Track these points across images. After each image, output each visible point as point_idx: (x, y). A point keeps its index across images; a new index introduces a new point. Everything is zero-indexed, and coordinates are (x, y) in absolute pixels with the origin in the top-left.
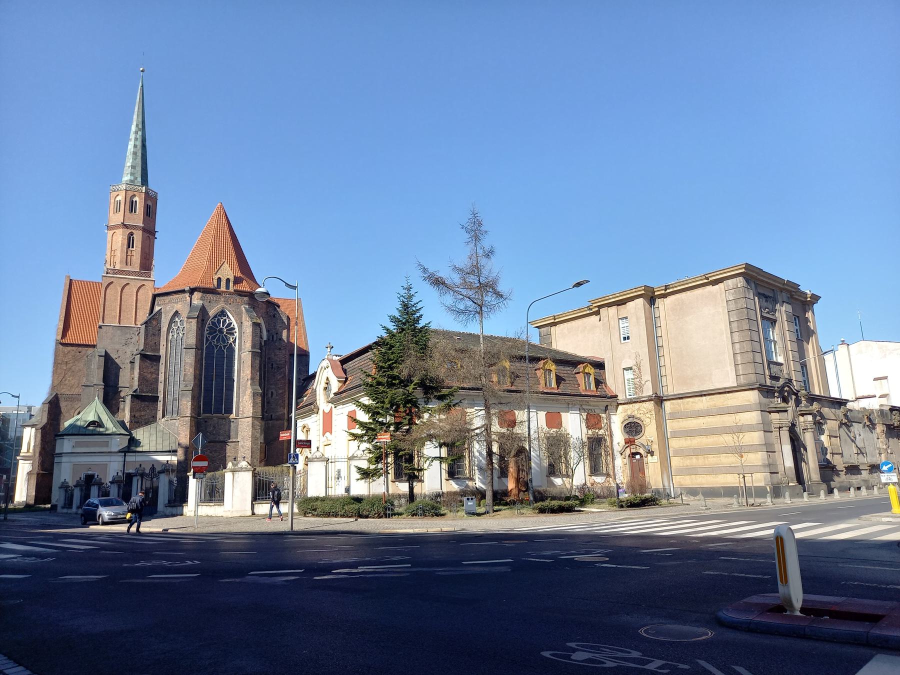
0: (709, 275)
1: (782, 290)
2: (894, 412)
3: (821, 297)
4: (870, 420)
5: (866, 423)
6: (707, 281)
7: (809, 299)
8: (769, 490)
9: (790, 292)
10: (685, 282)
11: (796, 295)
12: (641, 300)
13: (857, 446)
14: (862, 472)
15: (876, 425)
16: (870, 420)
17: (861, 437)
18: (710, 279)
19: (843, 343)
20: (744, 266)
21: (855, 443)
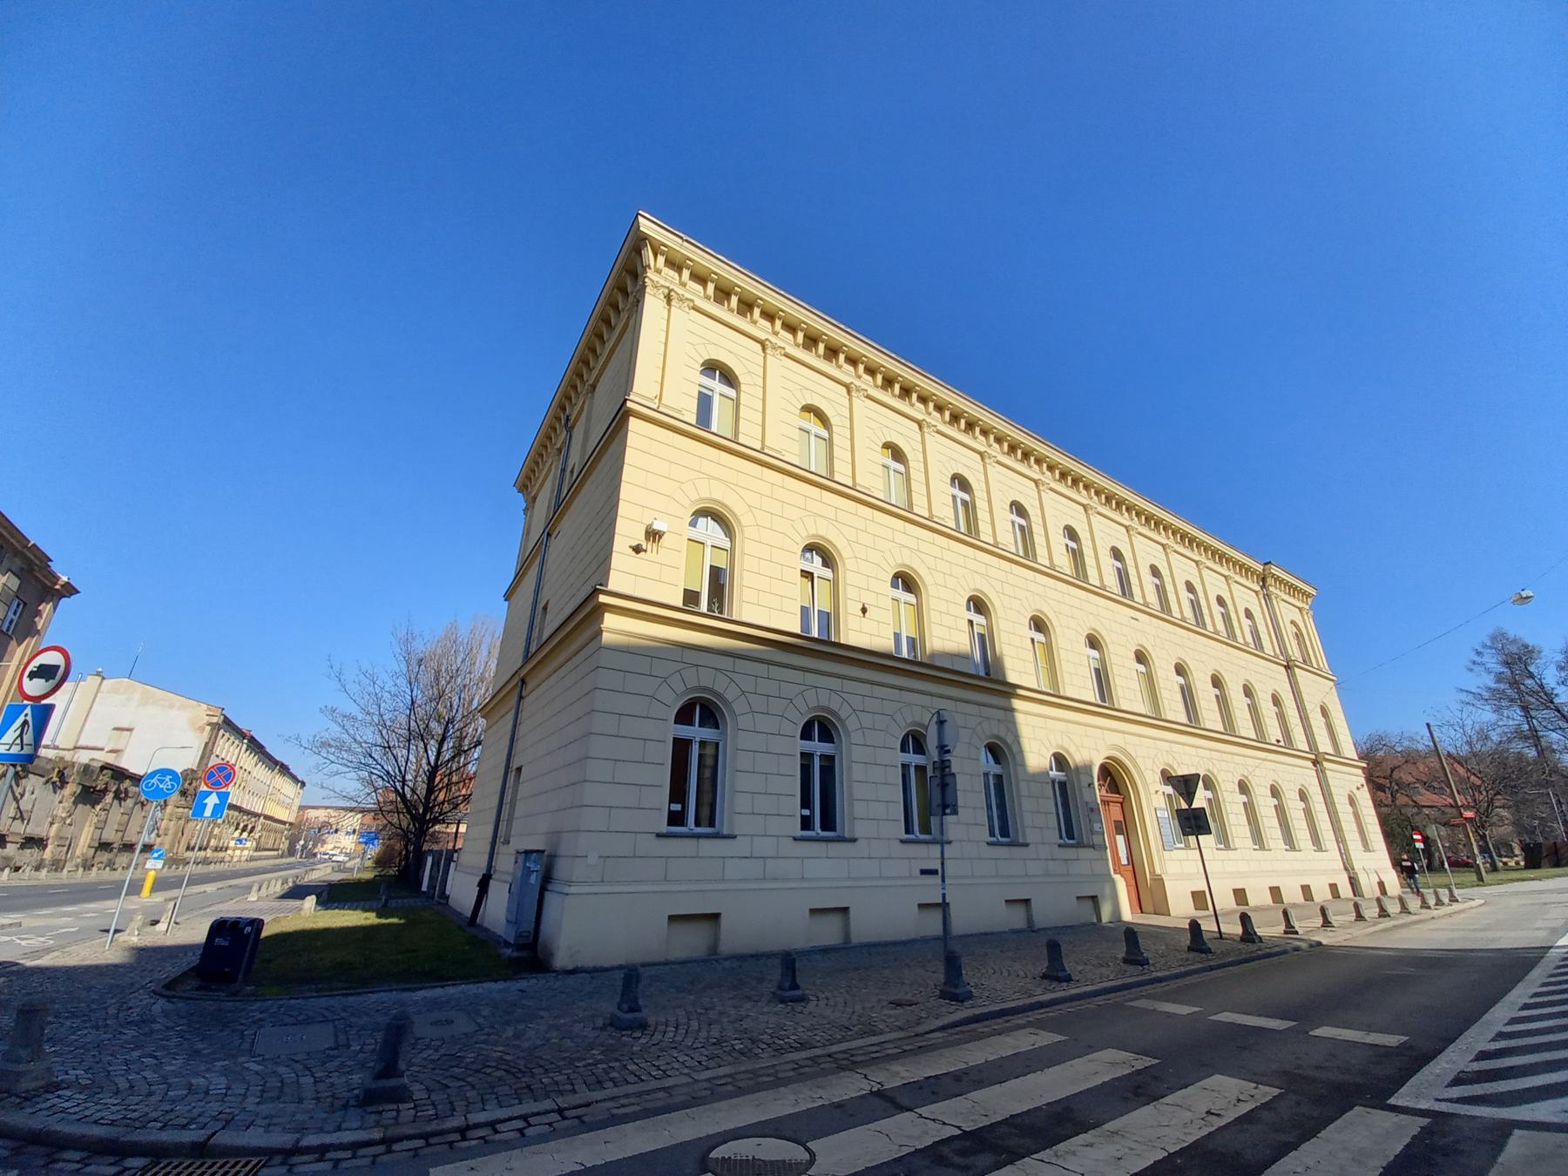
1: (16, 553)
2: (105, 772)
3: (78, 592)
4: (61, 774)
5: (52, 778)
7: (57, 587)
9: (30, 562)
11: (39, 571)
13: (18, 808)
14: (8, 845)
15: (67, 783)
16: (61, 774)
17: (34, 796)
19: (98, 674)
21: (18, 803)
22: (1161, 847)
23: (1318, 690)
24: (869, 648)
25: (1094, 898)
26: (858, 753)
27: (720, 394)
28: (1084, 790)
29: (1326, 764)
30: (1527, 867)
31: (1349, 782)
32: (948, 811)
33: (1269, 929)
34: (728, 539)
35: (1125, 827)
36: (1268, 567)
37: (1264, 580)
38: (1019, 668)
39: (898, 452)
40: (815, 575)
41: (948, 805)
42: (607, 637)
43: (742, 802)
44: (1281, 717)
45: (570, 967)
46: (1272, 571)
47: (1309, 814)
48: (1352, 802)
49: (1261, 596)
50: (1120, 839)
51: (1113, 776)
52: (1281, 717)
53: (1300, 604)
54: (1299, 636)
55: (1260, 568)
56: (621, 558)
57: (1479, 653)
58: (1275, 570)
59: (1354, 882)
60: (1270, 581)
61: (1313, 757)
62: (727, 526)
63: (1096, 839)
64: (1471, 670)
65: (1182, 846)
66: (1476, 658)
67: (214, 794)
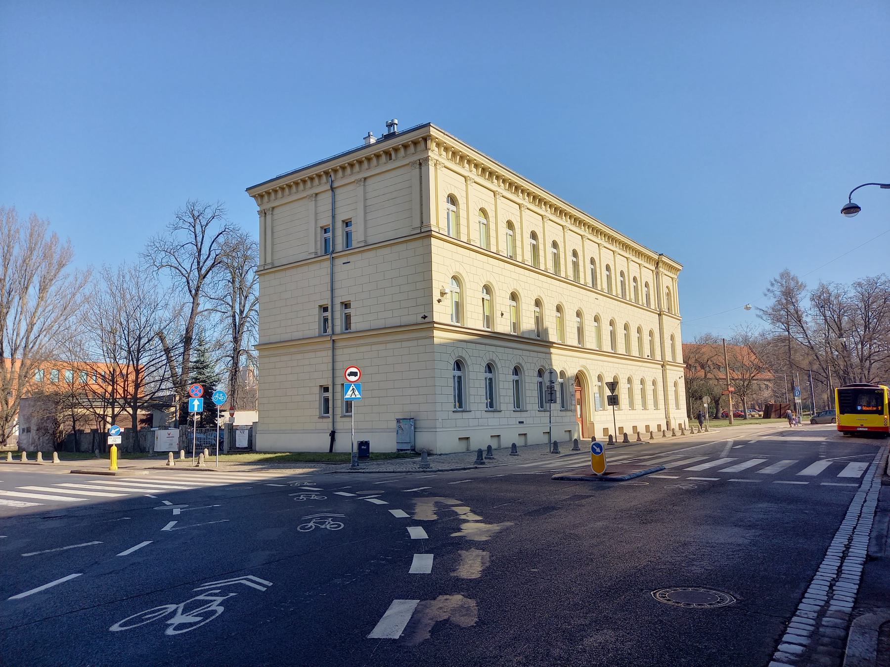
22: (594, 410)
23: (672, 326)
25: (570, 431)
29: (668, 367)
30: (764, 418)
31: (677, 375)
33: (632, 439)
35: (581, 402)
36: (661, 256)
37: (657, 264)
38: (553, 337)
42: (436, 341)
43: (472, 399)
44: (652, 343)
46: (663, 259)
47: (655, 391)
48: (675, 384)
49: (655, 273)
50: (578, 407)
51: (579, 379)
52: (652, 343)
53: (673, 276)
54: (668, 294)
55: (656, 257)
56: (436, 306)
57: (772, 285)
58: (664, 259)
59: (668, 424)
60: (660, 264)
61: (662, 363)
63: (573, 408)
64: (766, 295)
65: (602, 409)
66: (771, 288)
67: (196, 400)
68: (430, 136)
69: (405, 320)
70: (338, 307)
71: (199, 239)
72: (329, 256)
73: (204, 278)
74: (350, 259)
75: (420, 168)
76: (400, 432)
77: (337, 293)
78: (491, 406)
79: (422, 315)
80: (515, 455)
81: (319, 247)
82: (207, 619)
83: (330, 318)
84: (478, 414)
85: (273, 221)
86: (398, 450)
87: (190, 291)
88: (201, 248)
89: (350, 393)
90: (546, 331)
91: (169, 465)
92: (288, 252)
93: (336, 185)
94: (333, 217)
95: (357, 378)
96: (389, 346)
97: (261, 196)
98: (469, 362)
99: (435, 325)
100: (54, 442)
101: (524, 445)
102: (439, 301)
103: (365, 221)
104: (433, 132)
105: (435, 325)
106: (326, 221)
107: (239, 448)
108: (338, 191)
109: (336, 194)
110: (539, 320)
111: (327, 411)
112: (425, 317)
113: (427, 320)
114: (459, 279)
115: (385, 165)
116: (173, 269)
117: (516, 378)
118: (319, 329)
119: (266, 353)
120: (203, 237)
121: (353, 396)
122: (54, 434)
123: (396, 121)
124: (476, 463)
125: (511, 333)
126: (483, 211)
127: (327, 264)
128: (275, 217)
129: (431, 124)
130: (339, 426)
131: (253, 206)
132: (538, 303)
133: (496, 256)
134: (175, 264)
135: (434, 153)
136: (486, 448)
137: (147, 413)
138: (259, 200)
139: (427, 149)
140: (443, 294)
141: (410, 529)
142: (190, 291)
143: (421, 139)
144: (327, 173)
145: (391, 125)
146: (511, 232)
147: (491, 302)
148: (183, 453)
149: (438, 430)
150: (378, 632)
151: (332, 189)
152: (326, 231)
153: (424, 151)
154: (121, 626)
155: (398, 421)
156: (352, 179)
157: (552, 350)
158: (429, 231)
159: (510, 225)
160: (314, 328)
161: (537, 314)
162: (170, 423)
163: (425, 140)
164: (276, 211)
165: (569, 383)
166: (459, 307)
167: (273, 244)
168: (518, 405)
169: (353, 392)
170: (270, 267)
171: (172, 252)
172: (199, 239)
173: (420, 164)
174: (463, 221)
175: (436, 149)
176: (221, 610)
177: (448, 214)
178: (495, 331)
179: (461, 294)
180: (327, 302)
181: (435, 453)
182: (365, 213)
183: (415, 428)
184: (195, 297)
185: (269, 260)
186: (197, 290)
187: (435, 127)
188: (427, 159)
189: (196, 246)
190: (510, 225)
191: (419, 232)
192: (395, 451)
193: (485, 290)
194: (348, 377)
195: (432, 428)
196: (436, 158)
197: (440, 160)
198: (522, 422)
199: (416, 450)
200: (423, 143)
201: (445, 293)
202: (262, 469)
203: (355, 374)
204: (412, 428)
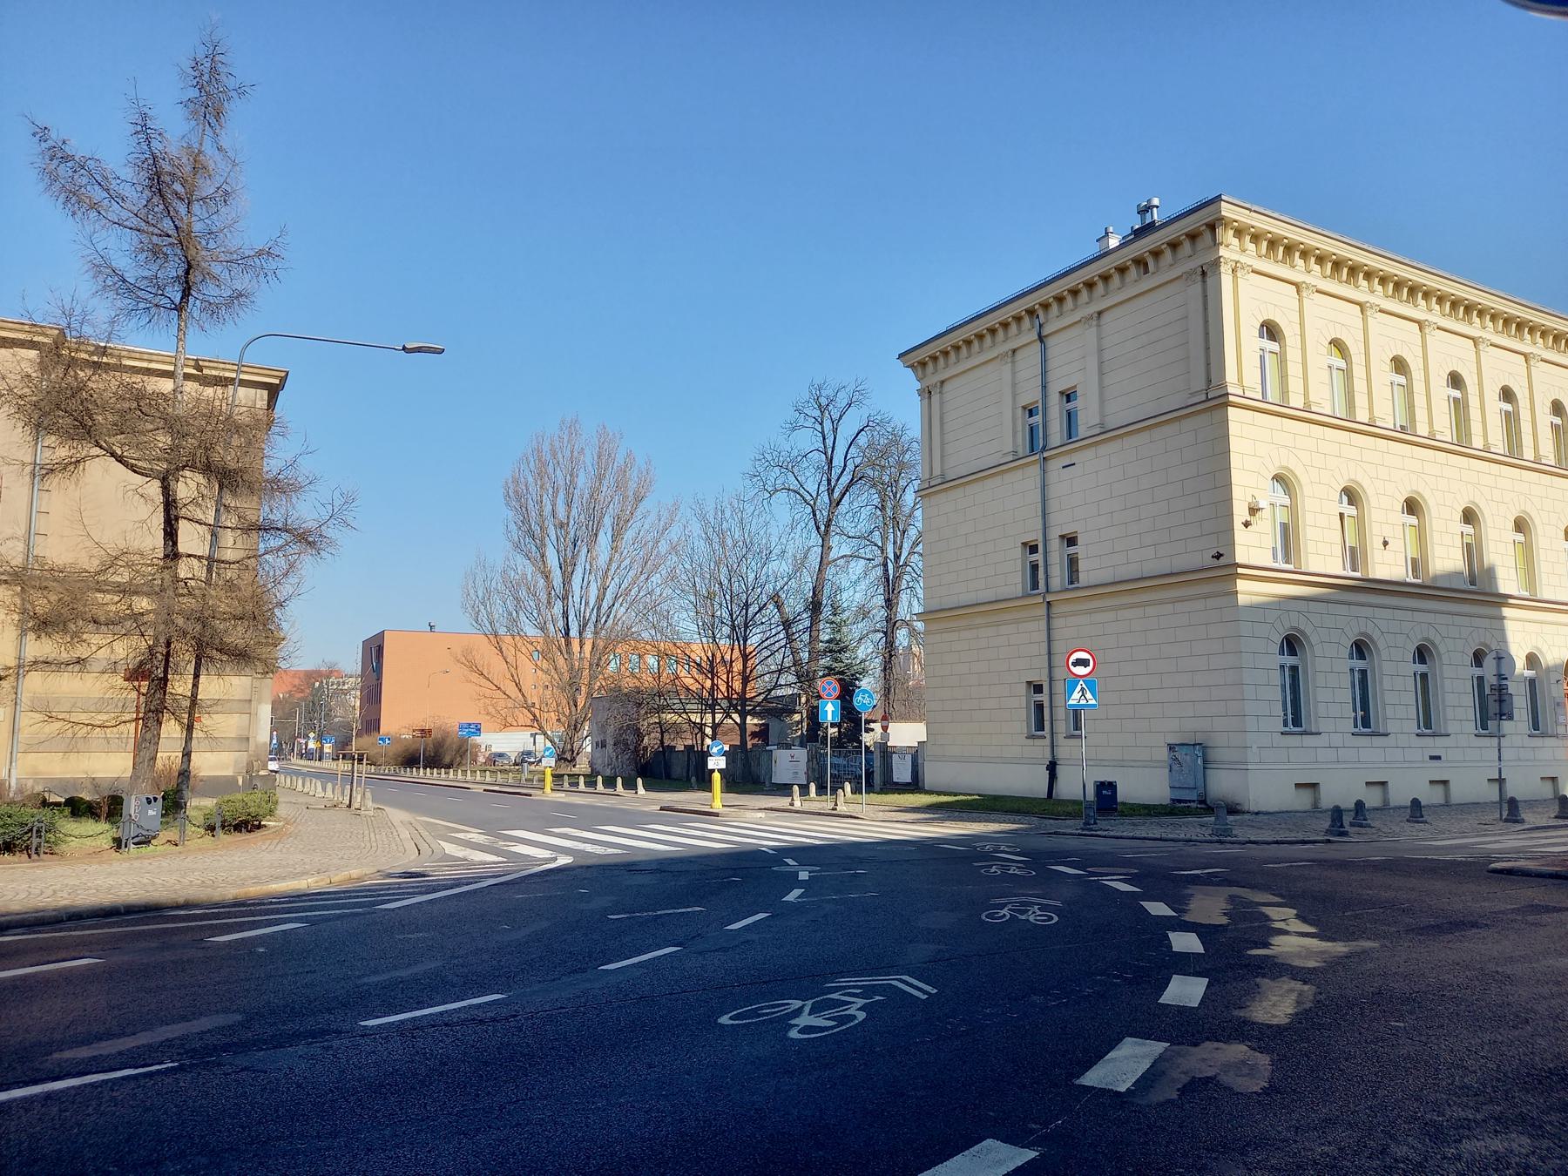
0: (207, 364)
6: (194, 372)
8: (240, 782)
10: (146, 357)
12: (33, 354)
18: (206, 371)
20: (283, 374)
24: (1389, 579)
26: (1388, 668)
27: (1270, 352)
28: (1552, 686)
32: (1504, 717)
34: (1287, 497)
38: (1507, 582)
39: (1400, 362)
40: (1346, 515)
41: (1505, 713)
42: (1242, 599)
45: (1256, 811)
56: (1240, 534)
62: (1287, 485)
67: (830, 704)
68: (1222, 218)
69: (1180, 563)
70: (1055, 544)
71: (829, 442)
72: (1037, 457)
73: (838, 504)
74: (1074, 458)
75: (1204, 282)
76: (1176, 767)
77: (1053, 519)
78: (1366, 722)
79: (1214, 552)
80: (1418, 822)
81: (1020, 441)
82: (842, 1025)
83: (1041, 564)
84: (1337, 740)
85: (942, 403)
86: (1173, 800)
87: (818, 528)
88: (832, 457)
89: (1076, 695)
90: (1490, 573)
91: (792, 805)
92: (964, 455)
93: (1045, 332)
94: (1044, 387)
95: (1087, 670)
96: (1151, 610)
97: (923, 364)
98: (1314, 639)
99: (1240, 570)
100: (636, 763)
101: (1443, 802)
102: (1247, 524)
103: (1102, 387)
104: (1227, 210)
105: (1240, 570)
106: (1031, 395)
107: (897, 783)
108: (1050, 342)
109: (1048, 346)
110: (1472, 551)
111: (1040, 727)
112: (1218, 556)
113: (1222, 561)
114: (1288, 481)
115: (1136, 283)
116: (792, 494)
117: (1421, 668)
118: (1023, 582)
119: (935, 626)
120: (835, 438)
121: (1083, 702)
122: (636, 751)
123: (1156, 201)
124: (1328, 832)
125: (1408, 580)
126: (1337, 344)
127: (1035, 471)
128: (947, 397)
129: (1223, 197)
130: (1062, 753)
131: (909, 381)
132: (1469, 516)
133: (1370, 430)
134: (794, 485)
135: (1230, 249)
136: (1352, 806)
137: (760, 722)
138: (919, 369)
139: (1216, 244)
140: (1253, 511)
141: (1172, 935)
142: (818, 528)
143: (1204, 227)
144: (1031, 312)
145: (1145, 210)
146: (1402, 380)
147: (1360, 521)
148: (813, 787)
149: (1249, 767)
150: (1093, 1077)
151: (1041, 338)
152: (1031, 414)
153: (1210, 247)
154: (731, 1018)
155: (1171, 747)
156: (1076, 317)
157: (1506, 611)
158: (1224, 395)
159: (1399, 365)
160: (1015, 581)
161: (1467, 540)
162: (793, 739)
163: (1212, 227)
164: (947, 387)
165: (1549, 679)
166: (1288, 537)
167: (943, 444)
168: (1427, 721)
169: (1083, 695)
170: (939, 481)
171: (789, 467)
172: (829, 442)
173: (1204, 273)
174: (1294, 369)
175: (1235, 241)
176: (861, 1016)
177: (1262, 358)
178: (1370, 577)
179: (1293, 510)
180: (1035, 536)
181: (1246, 808)
182: (1101, 373)
183: (1205, 761)
184: (825, 536)
185: (937, 472)
186: (828, 526)
187: (1230, 200)
188: (1216, 263)
189: (825, 454)
190: (1399, 365)
191: (1204, 398)
192: (1167, 801)
193: (1345, 499)
194: (1072, 668)
195: (1237, 763)
196: (1236, 257)
197: (1243, 259)
198: (1438, 758)
199: (1208, 803)
200: (1207, 235)
201: (1259, 510)
202: (933, 819)
203: (1084, 663)
204: (1199, 762)
